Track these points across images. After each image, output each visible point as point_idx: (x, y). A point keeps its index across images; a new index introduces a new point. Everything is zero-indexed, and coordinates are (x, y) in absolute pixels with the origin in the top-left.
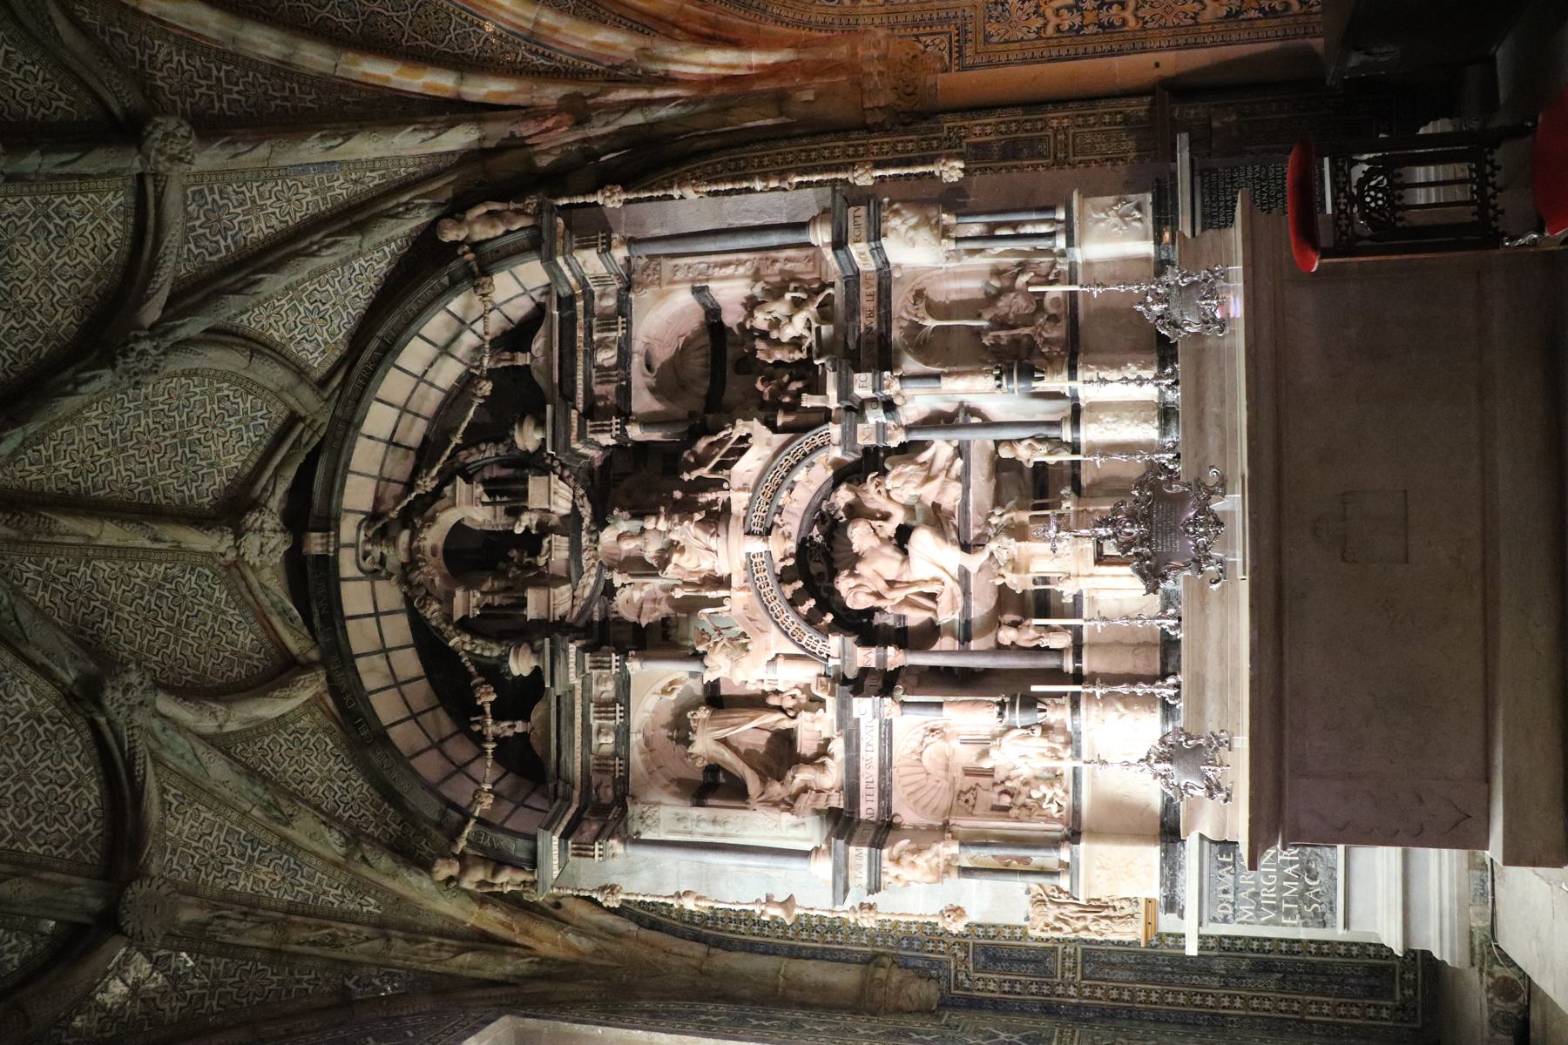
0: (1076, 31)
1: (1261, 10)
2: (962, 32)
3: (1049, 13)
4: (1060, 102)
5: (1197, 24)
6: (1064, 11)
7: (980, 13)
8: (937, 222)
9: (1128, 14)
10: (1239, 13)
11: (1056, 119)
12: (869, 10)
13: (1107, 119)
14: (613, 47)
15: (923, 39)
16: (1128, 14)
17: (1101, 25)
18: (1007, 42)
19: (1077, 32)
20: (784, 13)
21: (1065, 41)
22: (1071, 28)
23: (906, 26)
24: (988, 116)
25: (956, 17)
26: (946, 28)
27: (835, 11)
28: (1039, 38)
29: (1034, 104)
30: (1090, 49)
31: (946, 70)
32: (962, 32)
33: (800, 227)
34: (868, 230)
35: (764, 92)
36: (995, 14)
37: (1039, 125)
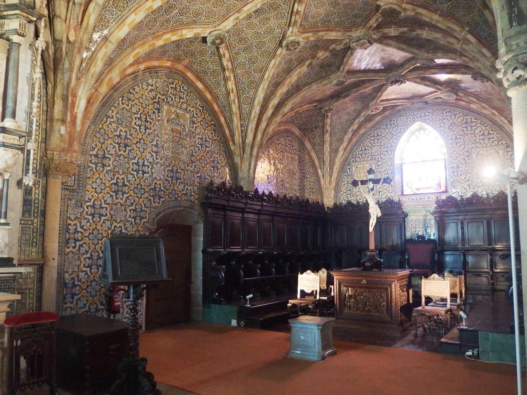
0: (68, 231)
1: (66, 295)
2: (74, 191)
3: (75, 222)
4: (43, 224)
5: (64, 272)
6: (75, 227)
7: (79, 198)
8: (6, 171)
9: (71, 249)
10: (66, 287)
11: (37, 221)
12: (87, 160)
13: (35, 240)
14: (95, 66)
15: (74, 177)
16: (71, 249)
17: (68, 239)
18: (68, 206)
19: (68, 231)
20: (91, 130)
21: (65, 227)
22: (69, 229)
23: (79, 171)
24: (42, 197)
25: (79, 189)
26: (76, 185)
27: (88, 148)
28: (67, 218)
29: (44, 214)
30: (61, 235)
31: (62, 184)
32: (74, 191)
33: (14, 116)
34: (8, 143)
35: (66, 116)
36: (78, 203)
37: (36, 215)
